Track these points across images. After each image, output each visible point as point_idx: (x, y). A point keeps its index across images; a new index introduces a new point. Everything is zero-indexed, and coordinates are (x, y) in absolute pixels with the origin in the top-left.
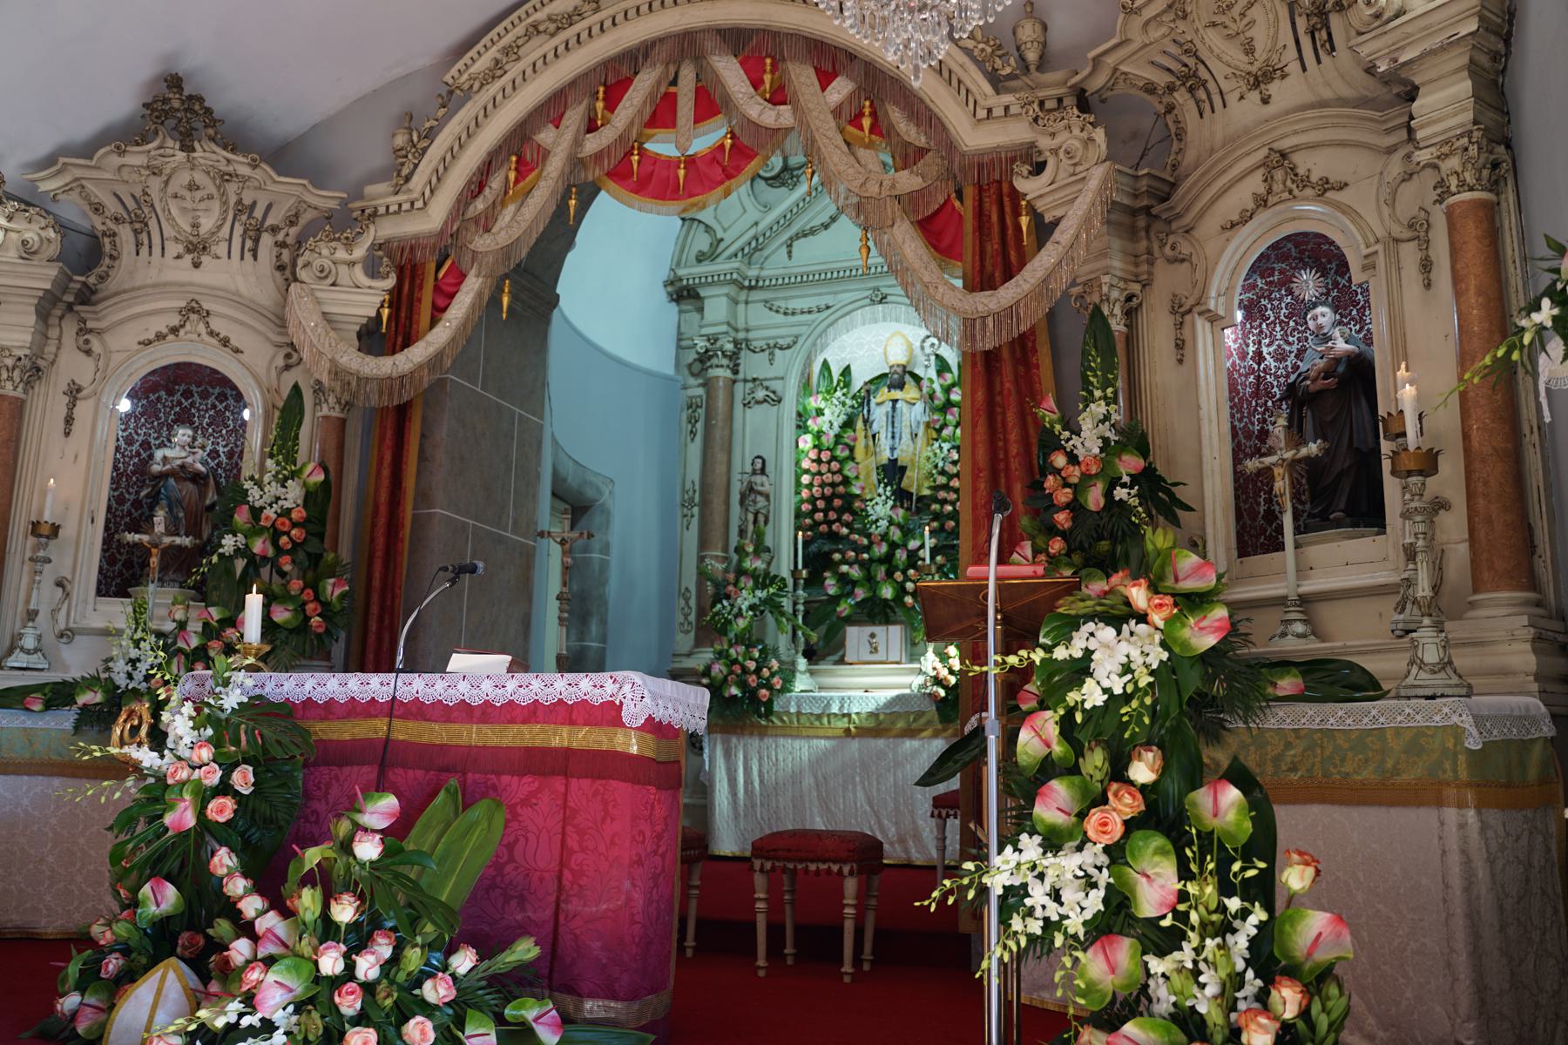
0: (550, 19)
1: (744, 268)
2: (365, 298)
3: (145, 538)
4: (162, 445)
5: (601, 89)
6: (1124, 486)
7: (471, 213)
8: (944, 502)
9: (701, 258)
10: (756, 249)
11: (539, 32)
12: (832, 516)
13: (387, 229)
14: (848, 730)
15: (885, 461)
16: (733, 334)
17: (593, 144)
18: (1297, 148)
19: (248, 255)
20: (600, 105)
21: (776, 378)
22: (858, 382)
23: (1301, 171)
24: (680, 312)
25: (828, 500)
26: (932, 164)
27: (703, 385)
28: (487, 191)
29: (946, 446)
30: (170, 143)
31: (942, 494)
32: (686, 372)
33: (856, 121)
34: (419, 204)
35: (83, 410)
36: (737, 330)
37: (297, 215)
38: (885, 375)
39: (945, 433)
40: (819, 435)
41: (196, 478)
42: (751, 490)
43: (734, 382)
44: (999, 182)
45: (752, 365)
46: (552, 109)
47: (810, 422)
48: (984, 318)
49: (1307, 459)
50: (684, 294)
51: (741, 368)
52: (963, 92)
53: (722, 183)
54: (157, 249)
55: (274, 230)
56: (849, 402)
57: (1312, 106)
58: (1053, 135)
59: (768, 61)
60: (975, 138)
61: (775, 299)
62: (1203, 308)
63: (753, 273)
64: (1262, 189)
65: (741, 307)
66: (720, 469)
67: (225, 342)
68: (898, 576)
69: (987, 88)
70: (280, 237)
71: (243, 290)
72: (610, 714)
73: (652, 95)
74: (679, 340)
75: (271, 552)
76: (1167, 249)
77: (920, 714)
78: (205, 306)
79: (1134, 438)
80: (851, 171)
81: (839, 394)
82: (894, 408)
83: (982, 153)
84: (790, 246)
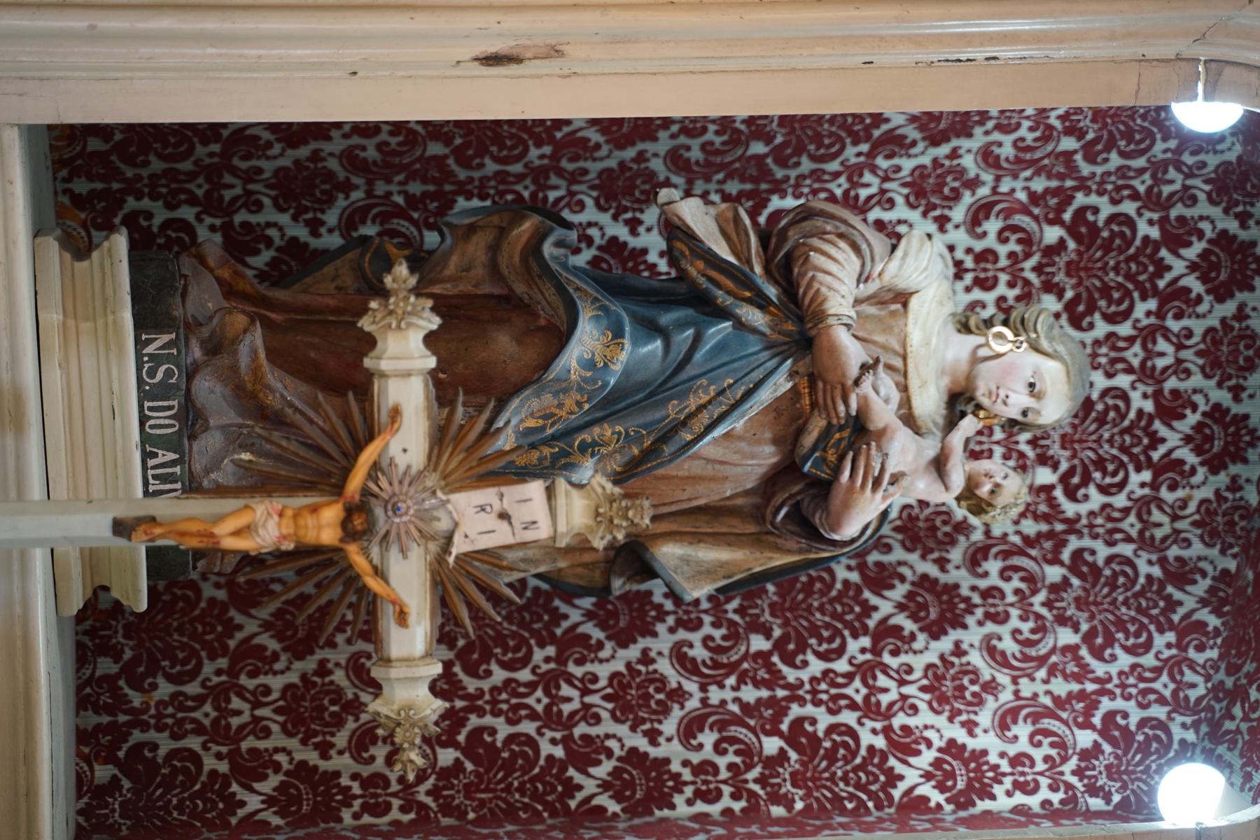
3: (407, 444)
4: (975, 270)
41: (800, 490)
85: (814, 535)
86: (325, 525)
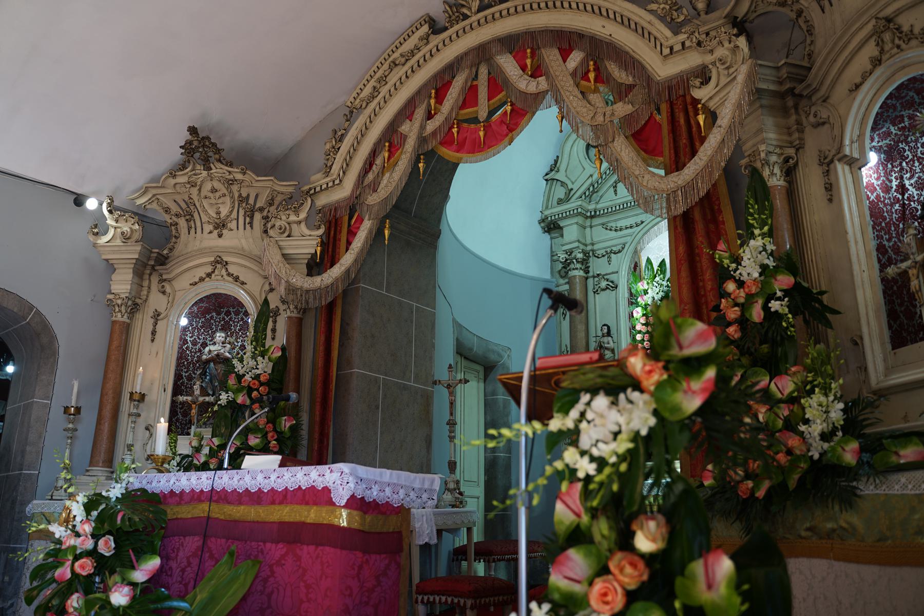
0: (402, 55)
1: (584, 204)
2: (307, 242)
3: (189, 398)
5: (433, 91)
6: (779, 299)
7: (366, 182)
9: (560, 202)
10: (594, 192)
11: (396, 65)
13: (323, 200)
16: (582, 247)
17: (431, 126)
18: (899, 12)
19: (248, 226)
20: (433, 101)
21: (613, 273)
23: (906, 28)
24: (551, 238)
26: (638, 94)
27: (568, 283)
28: (374, 166)
30: (198, 167)
32: (558, 276)
33: (585, 77)
34: (337, 182)
35: (161, 325)
36: (586, 245)
37: (272, 199)
40: (645, 307)
42: (601, 347)
43: (587, 278)
44: (684, 96)
45: (598, 266)
46: (406, 112)
47: (639, 300)
48: (675, 192)
50: (551, 227)
51: (590, 269)
52: (652, 39)
53: (507, 135)
54: (199, 230)
55: (261, 210)
56: (665, 283)
58: (711, 51)
59: (529, 51)
60: (664, 70)
61: (608, 222)
62: (840, 155)
63: (592, 207)
64: (876, 53)
65: (588, 230)
66: (581, 335)
69: (668, 33)
70: (265, 213)
71: (246, 247)
72: (320, 496)
73: (463, 89)
74: (552, 256)
75: (248, 402)
76: (812, 119)
78: (225, 259)
79: (790, 262)
80: (585, 110)
81: (657, 279)
83: (670, 79)
84: (616, 187)
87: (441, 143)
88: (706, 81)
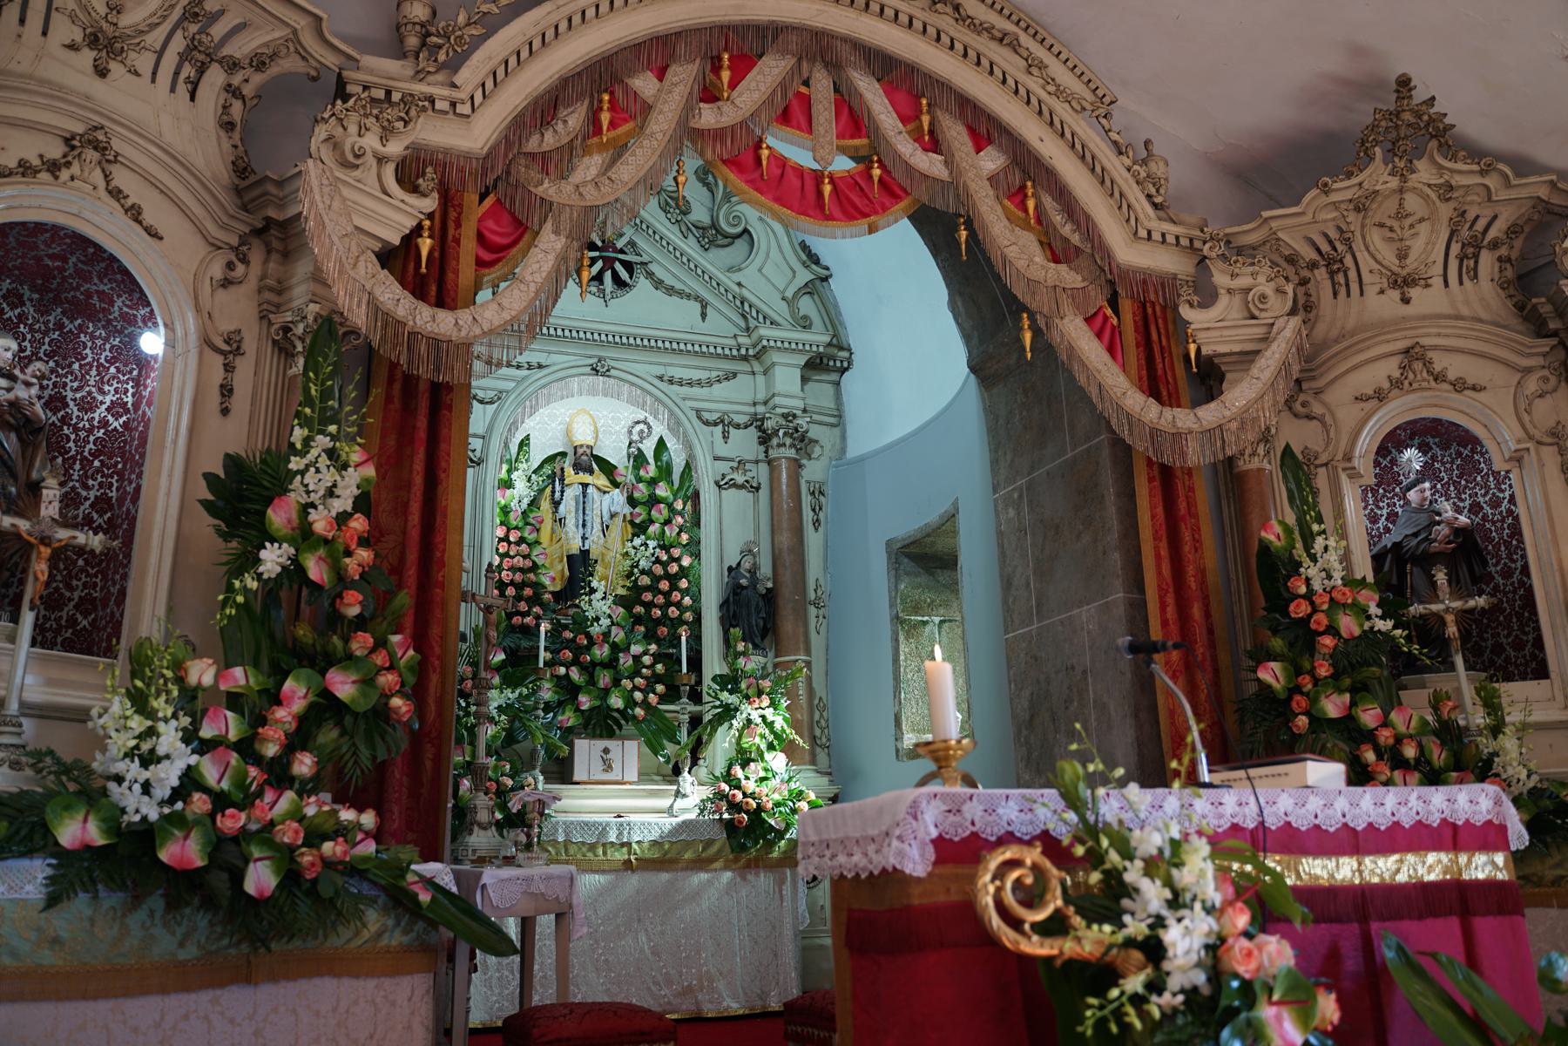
2: (398, 213)
3: (24, 525)
8: (649, 606)
12: (523, 606)
14: (627, 864)
15: (575, 551)
17: (708, 117)
18: (1435, 348)
19: (182, 89)
20: (726, 75)
22: (537, 456)
23: (1438, 367)
25: (519, 587)
29: (652, 544)
31: (648, 597)
34: (464, 109)
38: (563, 454)
39: (651, 529)
40: (505, 510)
49: (1471, 611)
52: (1125, 207)
55: (232, 65)
57: (1449, 317)
58: (1233, 276)
59: (924, 102)
64: (1397, 374)
67: (135, 213)
68: (627, 683)
70: (236, 80)
73: (783, 85)
77: (708, 844)
78: (116, 144)
82: (584, 494)
85: (41, 429)
86: (46, 552)
87: (725, 162)
88: (1204, 305)
